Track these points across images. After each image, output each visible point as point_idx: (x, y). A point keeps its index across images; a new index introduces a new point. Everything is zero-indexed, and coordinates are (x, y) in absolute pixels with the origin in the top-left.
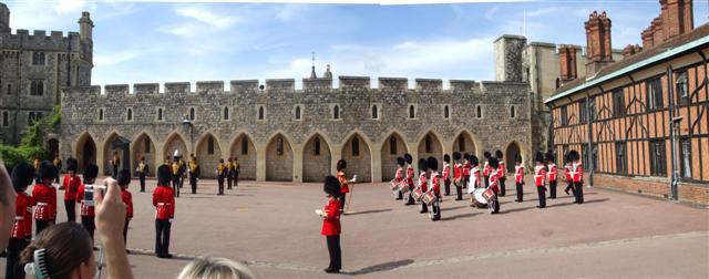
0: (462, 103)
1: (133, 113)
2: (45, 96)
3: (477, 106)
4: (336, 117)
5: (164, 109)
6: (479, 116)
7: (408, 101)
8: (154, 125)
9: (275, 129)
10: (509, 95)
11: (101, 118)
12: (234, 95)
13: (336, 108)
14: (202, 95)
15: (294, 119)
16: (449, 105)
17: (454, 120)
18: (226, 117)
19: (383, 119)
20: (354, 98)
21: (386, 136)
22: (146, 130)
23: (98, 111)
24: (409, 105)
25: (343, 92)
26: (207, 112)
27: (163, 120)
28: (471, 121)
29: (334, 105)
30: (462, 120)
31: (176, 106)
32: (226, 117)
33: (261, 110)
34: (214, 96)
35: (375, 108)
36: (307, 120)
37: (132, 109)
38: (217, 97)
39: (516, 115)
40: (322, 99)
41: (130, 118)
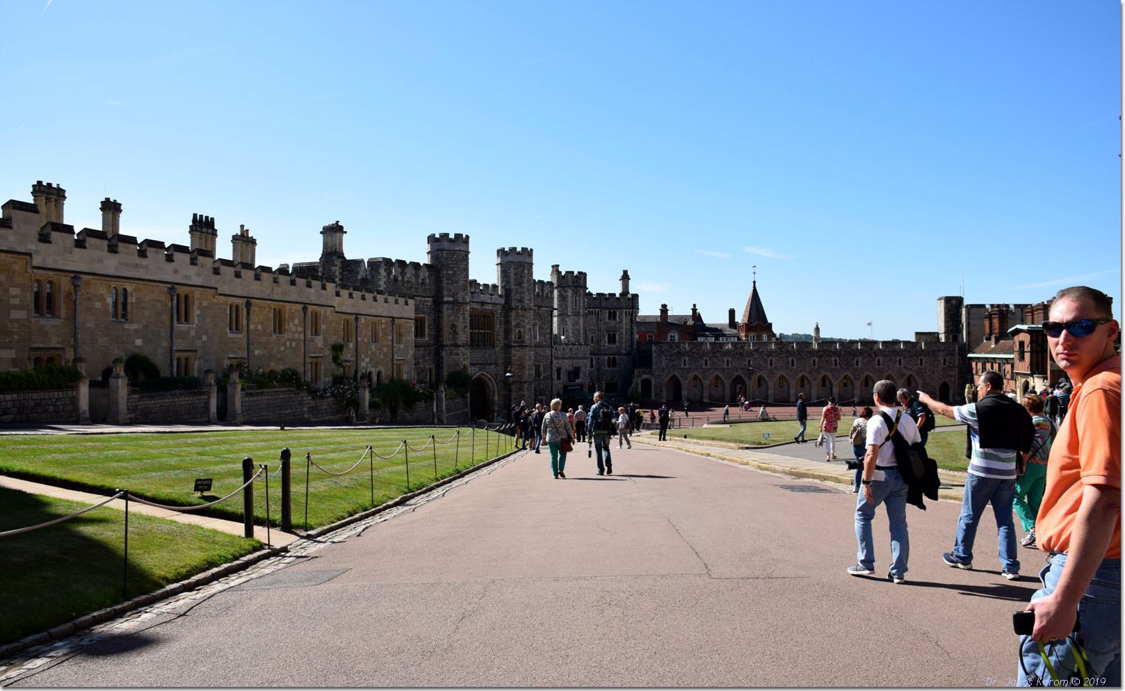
1: (708, 362)
2: (618, 344)
3: (920, 358)
4: (836, 365)
5: (730, 359)
6: (921, 364)
7: (876, 355)
8: (723, 370)
9: (801, 372)
11: (685, 365)
12: (776, 351)
13: (836, 361)
14: (756, 350)
16: (902, 358)
17: (905, 367)
18: (771, 365)
20: (846, 355)
21: (863, 377)
22: (717, 373)
31: (739, 358)
32: (771, 365)
34: (763, 352)
35: (857, 362)
36: (819, 367)
37: (707, 358)
38: (766, 353)
39: (947, 364)
41: (706, 365)
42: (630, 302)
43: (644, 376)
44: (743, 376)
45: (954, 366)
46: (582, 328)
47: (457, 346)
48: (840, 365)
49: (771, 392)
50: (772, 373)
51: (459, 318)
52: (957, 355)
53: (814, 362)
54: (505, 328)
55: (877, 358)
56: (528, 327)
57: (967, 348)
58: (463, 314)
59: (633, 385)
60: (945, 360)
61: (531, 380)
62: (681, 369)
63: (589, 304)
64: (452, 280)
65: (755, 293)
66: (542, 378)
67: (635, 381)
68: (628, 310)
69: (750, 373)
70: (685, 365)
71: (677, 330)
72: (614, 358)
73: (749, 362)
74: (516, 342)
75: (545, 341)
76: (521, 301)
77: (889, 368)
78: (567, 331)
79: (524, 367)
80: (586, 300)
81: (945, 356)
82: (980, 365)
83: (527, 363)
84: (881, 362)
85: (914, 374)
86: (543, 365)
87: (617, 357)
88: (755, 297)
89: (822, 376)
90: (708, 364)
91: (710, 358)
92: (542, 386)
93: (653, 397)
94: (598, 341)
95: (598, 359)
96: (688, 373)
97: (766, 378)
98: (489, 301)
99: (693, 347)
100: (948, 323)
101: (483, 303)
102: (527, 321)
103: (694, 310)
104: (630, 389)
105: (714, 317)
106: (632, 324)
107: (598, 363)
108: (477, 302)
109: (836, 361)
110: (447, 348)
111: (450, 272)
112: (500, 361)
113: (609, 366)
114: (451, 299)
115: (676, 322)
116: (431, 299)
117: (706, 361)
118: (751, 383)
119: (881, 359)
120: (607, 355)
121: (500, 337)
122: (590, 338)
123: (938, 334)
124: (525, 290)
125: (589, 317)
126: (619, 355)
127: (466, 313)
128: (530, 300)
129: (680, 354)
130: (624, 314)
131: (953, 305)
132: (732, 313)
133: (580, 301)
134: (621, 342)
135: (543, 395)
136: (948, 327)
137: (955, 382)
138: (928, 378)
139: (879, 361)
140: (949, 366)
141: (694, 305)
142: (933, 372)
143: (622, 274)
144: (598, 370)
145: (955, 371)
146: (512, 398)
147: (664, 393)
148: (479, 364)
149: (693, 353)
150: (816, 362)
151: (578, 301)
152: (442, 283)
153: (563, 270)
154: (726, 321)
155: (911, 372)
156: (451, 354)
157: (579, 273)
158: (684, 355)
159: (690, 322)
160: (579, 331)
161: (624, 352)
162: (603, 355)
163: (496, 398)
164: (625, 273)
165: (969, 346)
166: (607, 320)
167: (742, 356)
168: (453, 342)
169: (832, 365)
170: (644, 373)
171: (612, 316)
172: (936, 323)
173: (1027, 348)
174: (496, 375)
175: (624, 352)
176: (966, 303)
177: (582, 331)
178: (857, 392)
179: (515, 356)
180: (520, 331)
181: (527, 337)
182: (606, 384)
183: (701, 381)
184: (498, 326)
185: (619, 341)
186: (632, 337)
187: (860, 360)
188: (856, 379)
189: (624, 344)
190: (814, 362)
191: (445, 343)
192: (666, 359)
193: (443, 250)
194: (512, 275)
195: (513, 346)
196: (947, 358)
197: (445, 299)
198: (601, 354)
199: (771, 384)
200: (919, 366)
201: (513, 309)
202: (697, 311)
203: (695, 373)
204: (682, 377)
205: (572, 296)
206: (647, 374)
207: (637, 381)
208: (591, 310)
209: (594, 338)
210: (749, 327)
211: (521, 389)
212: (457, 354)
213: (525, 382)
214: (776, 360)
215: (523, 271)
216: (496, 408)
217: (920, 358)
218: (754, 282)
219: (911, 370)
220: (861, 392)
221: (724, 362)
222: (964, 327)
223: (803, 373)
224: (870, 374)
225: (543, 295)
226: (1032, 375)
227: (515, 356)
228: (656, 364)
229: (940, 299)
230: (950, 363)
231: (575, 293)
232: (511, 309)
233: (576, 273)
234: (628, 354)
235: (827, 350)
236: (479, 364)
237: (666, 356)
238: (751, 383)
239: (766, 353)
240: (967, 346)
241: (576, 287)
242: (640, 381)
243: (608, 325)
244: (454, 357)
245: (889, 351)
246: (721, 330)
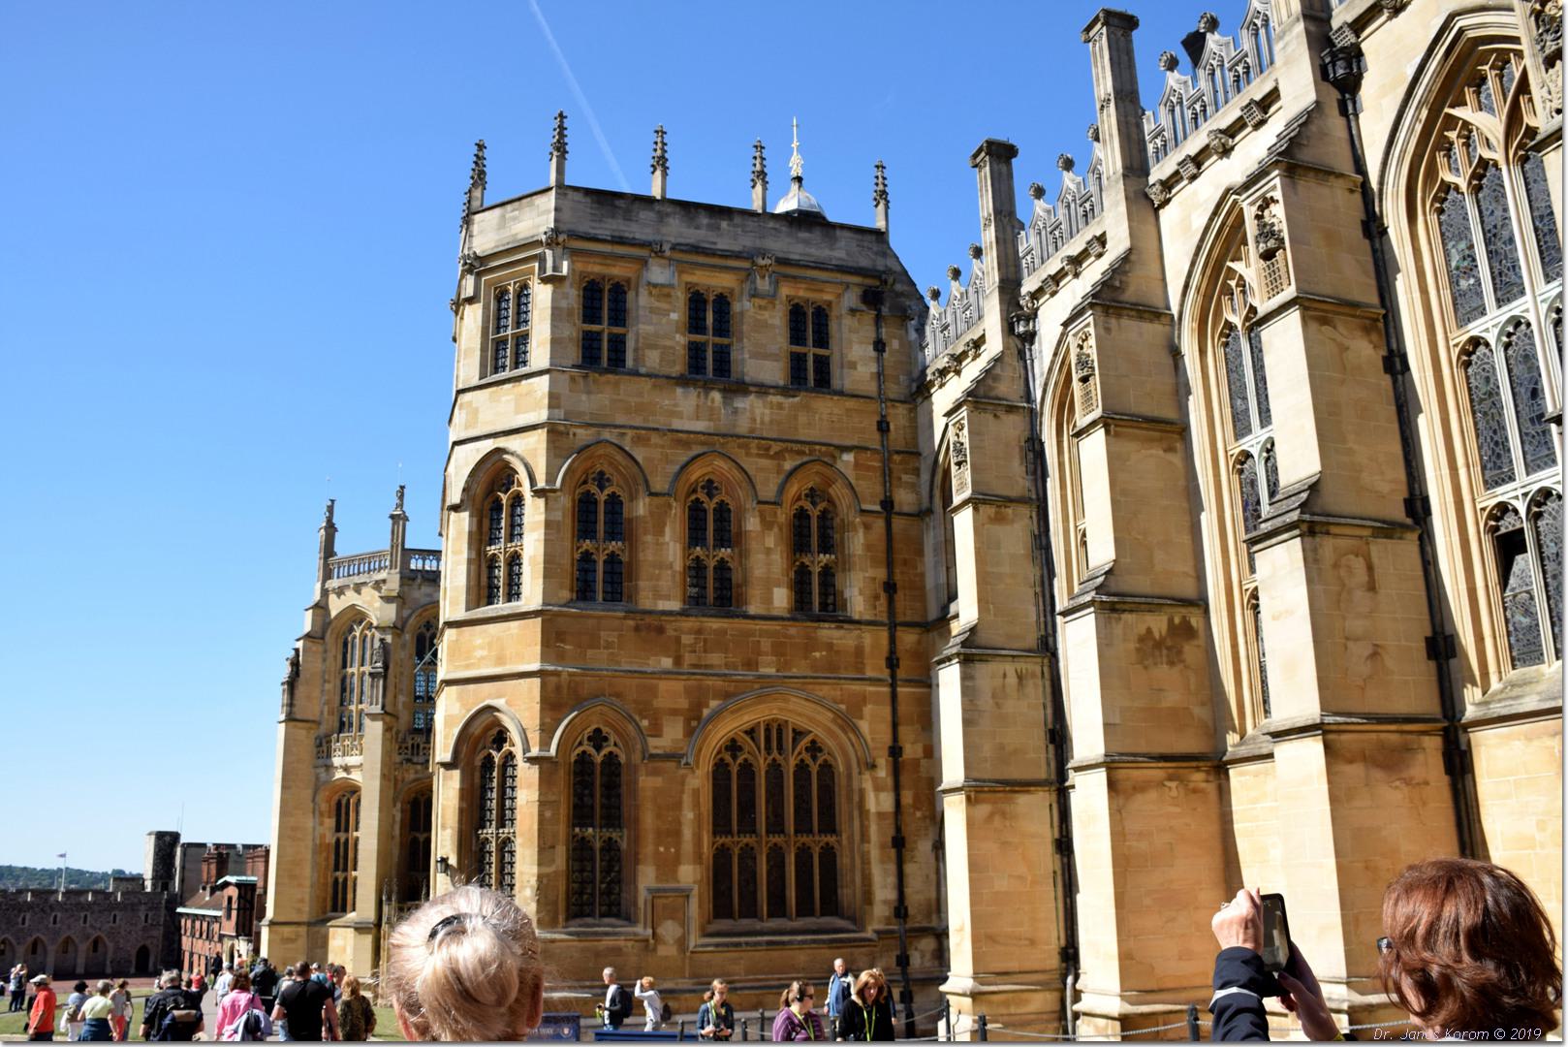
0: (100, 912)
6: (114, 922)
28: (107, 926)
30: (98, 925)
39: (149, 921)
57: (179, 899)
60: (147, 916)
82: (189, 923)
85: (103, 935)
131: (166, 843)
138: (121, 941)
140: (152, 925)
142: (130, 933)
155: (99, 933)
165: (181, 897)
172: (141, 863)
173: (235, 906)
176: (183, 840)
200: (111, 924)
226: (237, 937)
229: (150, 834)
230: (153, 920)
240: (179, 899)
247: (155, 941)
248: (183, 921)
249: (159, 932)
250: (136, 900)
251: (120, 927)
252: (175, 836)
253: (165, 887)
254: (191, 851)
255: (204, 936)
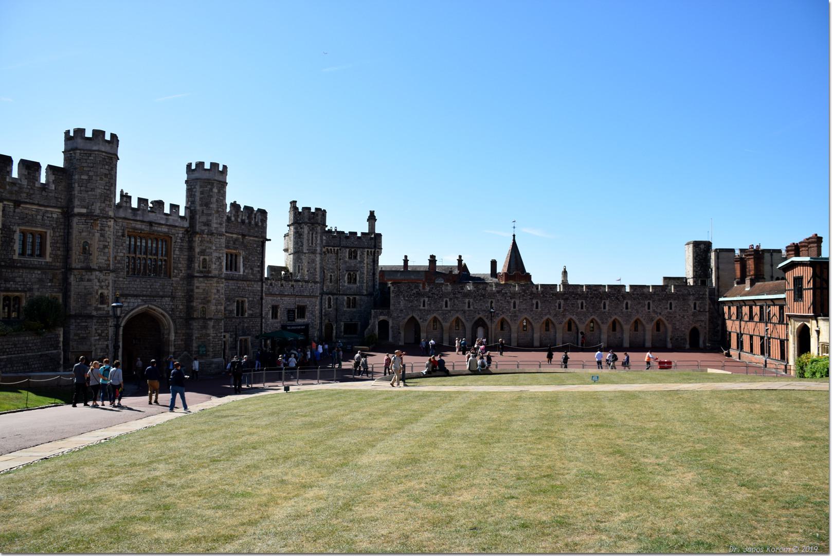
0: (659, 300)
1: (449, 303)
3: (669, 302)
4: (582, 308)
5: (471, 300)
6: (671, 309)
8: (464, 312)
9: (546, 315)
10: (693, 294)
11: (424, 306)
12: (519, 293)
13: (582, 304)
14: (498, 292)
15: (557, 309)
16: (651, 302)
17: (654, 311)
18: (514, 307)
19: (609, 310)
20: (592, 298)
21: (610, 320)
23: (422, 301)
24: (625, 302)
25: (587, 294)
26: (501, 303)
27: (471, 308)
29: (581, 301)
30: (659, 311)
32: (514, 307)
33: (537, 303)
34: (506, 293)
36: (565, 310)
37: (448, 299)
38: (509, 294)
39: (698, 308)
40: (574, 297)
41: (446, 306)
42: (373, 241)
43: (382, 318)
44: (485, 319)
45: (704, 311)
46: (318, 266)
47: (89, 269)
48: (587, 309)
49: (514, 335)
50: (515, 316)
51: (94, 235)
52: (707, 300)
53: (560, 305)
54: (189, 256)
55: (625, 302)
56: (215, 254)
58: (101, 230)
59: (369, 327)
60: (695, 304)
61: (220, 316)
62: (420, 310)
63: (327, 243)
64: (86, 187)
65: (514, 246)
66: (246, 315)
67: (371, 321)
68: (370, 250)
69: (492, 316)
70: (424, 306)
71: (442, 278)
72: (355, 298)
73: (492, 302)
74: (201, 272)
75: (252, 274)
76: (207, 224)
77: (638, 312)
78: (302, 269)
79: (209, 301)
80: (324, 238)
81: (695, 300)
82: (734, 309)
83: (213, 296)
84: (629, 306)
85: (663, 319)
86: (249, 302)
87: (357, 297)
88: (515, 249)
89: (567, 319)
90: (449, 305)
91: (450, 299)
92: (246, 325)
93: (390, 339)
94: (337, 281)
95: (337, 299)
96: (428, 315)
97: (509, 321)
98: (163, 222)
99: (433, 288)
100: (697, 268)
101: (151, 224)
102: (214, 248)
103: (460, 261)
104: (367, 330)
105: (478, 267)
106: (374, 264)
107: (336, 303)
108: (142, 221)
109: (582, 304)
110: (76, 272)
111: (85, 177)
112: (180, 294)
113: (349, 307)
114: (84, 211)
115: (444, 272)
116: (59, 210)
117: (446, 303)
118: (493, 326)
119: (629, 302)
120: (346, 295)
121: (180, 265)
122: (329, 277)
123: (686, 279)
124: (214, 212)
125: (329, 255)
126: (358, 295)
127: (107, 229)
128: (221, 224)
129: (419, 294)
130: (366, 253)
131: (701, 250)
132: (494, 264)
133: (316, 237)
134: (362, 282)
135: (248, 335)
136: (696, 272)
137: (705, 327)
139: (627, 304)
140: (699, 311)
141: (460, 257)
142: (683, 317)
143: (369, 214)
144: (337, 310)
145: (706, 315)
146: (194, 338)
147: (402, 334)
148: (143, 296)
149: (432, 294)
150: (562, 306)
151: (314, 238)
152: (74, 190)
153: (300, 206)
154: (488, 271)
155: (660, 317)
156: (82, 280)
157: (317, 209)
158: (423, 296)
159: (456, 272)
160: (315, 269)
161: (365, 292)
162: (342, 295)
163: (172, 337)
164: (372, 213)
165: (718, 291)
166: (347, 259)
167: (484, 298)
168: (83, 265)
169: (579, 308)
170: (381, 314)
171: (353, 255)
172: (685, 269)
174: (173, 310)
175: (365, 292)
176: (714, 247)
177: (318, 270)
178: (604, 337)
179: (198, 288)
180: (204, 260)
181: (214, 266)
182: (345, 324)
183: (441, 324)
184: (177, 252)
185: (359, 281)
186: (374, 277)
187: (607, 303)
188: (602, 323)
189: (365, 284)
190: (560, 305)
191: (74, 266)
192: (405, 299)
193: (76, 149)
194: (198, 194)
195: (196, 277)
196: (698, 303)
197: (76, 210)
198: (340, 294)
199: (514, 328)
200: (669, 310)
201: (197, 233)
202: (463, 262)
203: (435, 315)
204: (420, 319)
205: (309, 233)
206: (384, 315)
207: (374, 326)
208: (329, 248)
209: (333, 277)
210: (508, 276)
211: (205, 327)
212: (89, 280)
213: (211, 319)
214: (520, 302)
215: (211, 190)
216: (172, 349)
217: (669, 302)
218: (514, 236)
219: (660, 314)
220: (609, 336)
221: (465, 303)
222: (714, 271)
223: (548, 316)
224: (617, 318)
225: (250, 223)
227: (198, 288)
228: (394, 305)
229: (688, 244)
230: (700, 308)
231: (312, 230)
232: (195, 233)
233: (313, 210)
234: (370, 294)
235: (573, 293)
236: (143, 296)
237: (404, 297)
238: (494, 326)
239: (509, 294)
241: (313, 224)
242: (377, 323)
243: (348, 265)
244: (86, 283)
245: (638, 294)
246: (483, 279)
247: (703, 324)
248: (726, 309)
249: (705, 317)
250: (686, 292)
251: (675, 312)
252: (708, 244)
253: (704, 283)
254: (722, 255)
255: (757, 319)
